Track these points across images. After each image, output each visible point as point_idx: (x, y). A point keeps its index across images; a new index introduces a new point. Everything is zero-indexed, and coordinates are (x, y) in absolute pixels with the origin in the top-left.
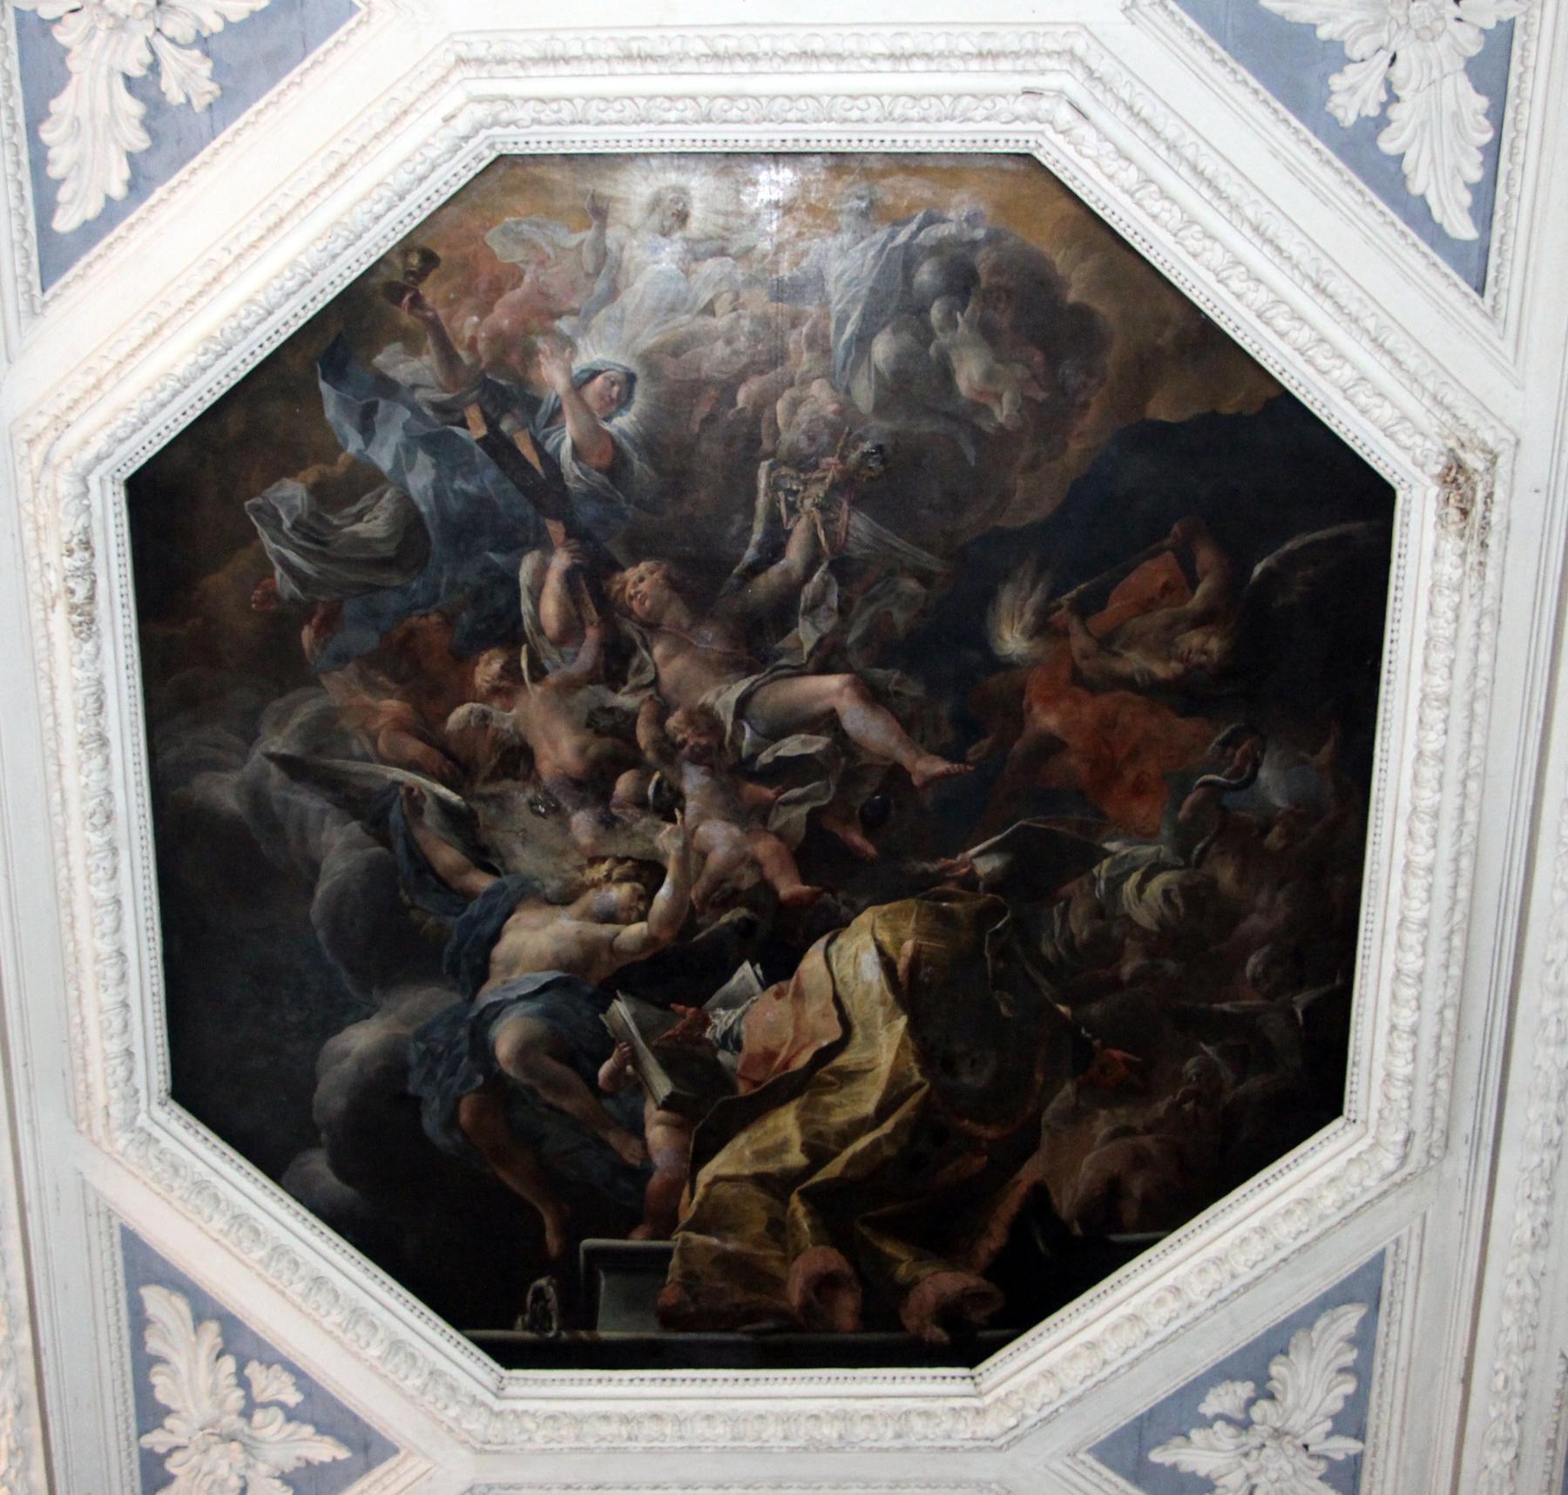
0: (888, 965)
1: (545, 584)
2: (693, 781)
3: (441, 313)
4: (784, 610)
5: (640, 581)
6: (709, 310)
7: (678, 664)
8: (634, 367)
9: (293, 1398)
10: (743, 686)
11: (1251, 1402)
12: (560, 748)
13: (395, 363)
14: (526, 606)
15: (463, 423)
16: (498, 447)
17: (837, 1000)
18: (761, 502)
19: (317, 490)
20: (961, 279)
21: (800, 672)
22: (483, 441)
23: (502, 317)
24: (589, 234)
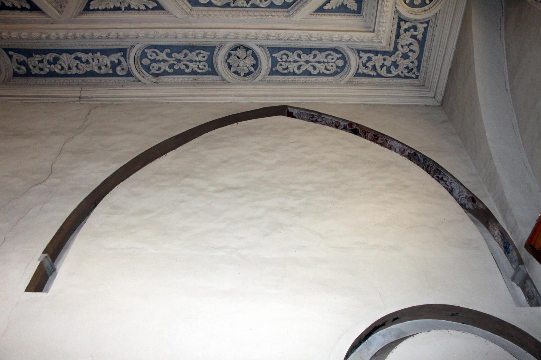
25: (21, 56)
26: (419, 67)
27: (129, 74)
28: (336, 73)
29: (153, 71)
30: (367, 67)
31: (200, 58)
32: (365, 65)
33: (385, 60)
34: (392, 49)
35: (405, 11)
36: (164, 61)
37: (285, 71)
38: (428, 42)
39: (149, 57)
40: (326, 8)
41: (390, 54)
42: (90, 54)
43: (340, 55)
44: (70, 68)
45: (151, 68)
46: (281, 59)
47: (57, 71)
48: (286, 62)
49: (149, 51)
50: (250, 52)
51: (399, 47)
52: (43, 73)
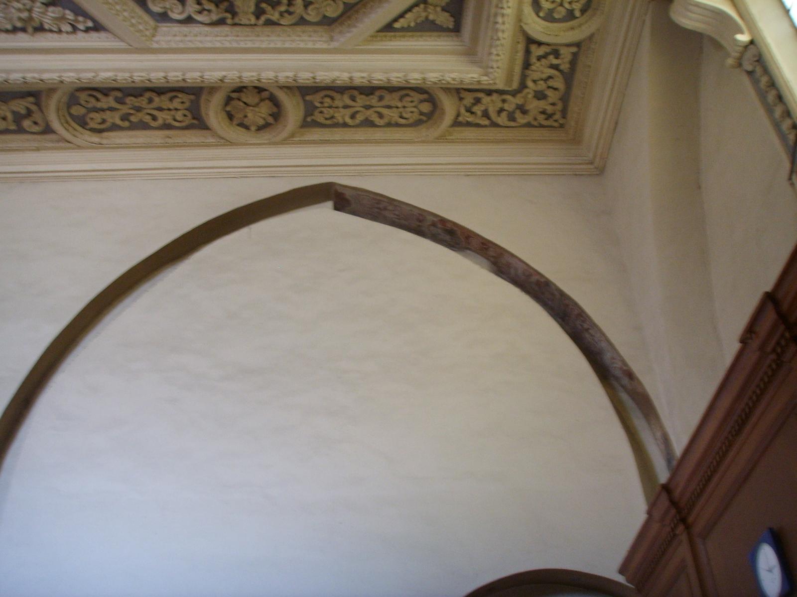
26: (564, 113)
27: (48, 130)
28: (417, 123)
29: (92, 125)
30: (472, 113)
31: (176, 104)
32: (469, 110)
33: (504, 101)
34: (515, 85)
35: (537, 27)
36: (111, 109)
37: (328, 122)
38: (579, 76)
39: (83, 103)
40: (397, 25)
41: (514, 93)
43: (425, 96)
45: (88, 120)
46: (322, 103)
48: (330, 107)
49: (83, 96)
50: (265, 94)
51: (530, 84)
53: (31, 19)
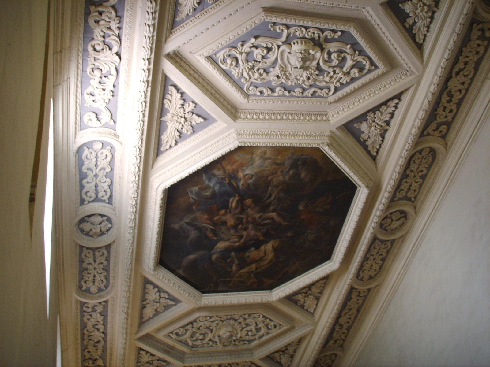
0: (273, 246)
1: (233, 202)
2: (250, 226)
3: (225, 166)
4: (269, 205)
5: (248, 201)
6: (267, 167)
7: (252, 212)
8: (254, 174)
9: (167, 297)
10: (260, 214)
11: (307, 291)
12: (231, 221)
13: (216, 172)
14: (230, 204)
15: (225, 181)
16: (230, 184)
17: (265, 252)
18: (269, 192)
19: (200, 189)
20: (304, 163)
21: (269, 212)
22: (228, 183)
23: (234, 167)
24: (250, 156)
25: (432, 125)
42: (461, 58)
44: (463, 83)
47: (460, 97)
52: (455, 111)
53: (429, 6)
